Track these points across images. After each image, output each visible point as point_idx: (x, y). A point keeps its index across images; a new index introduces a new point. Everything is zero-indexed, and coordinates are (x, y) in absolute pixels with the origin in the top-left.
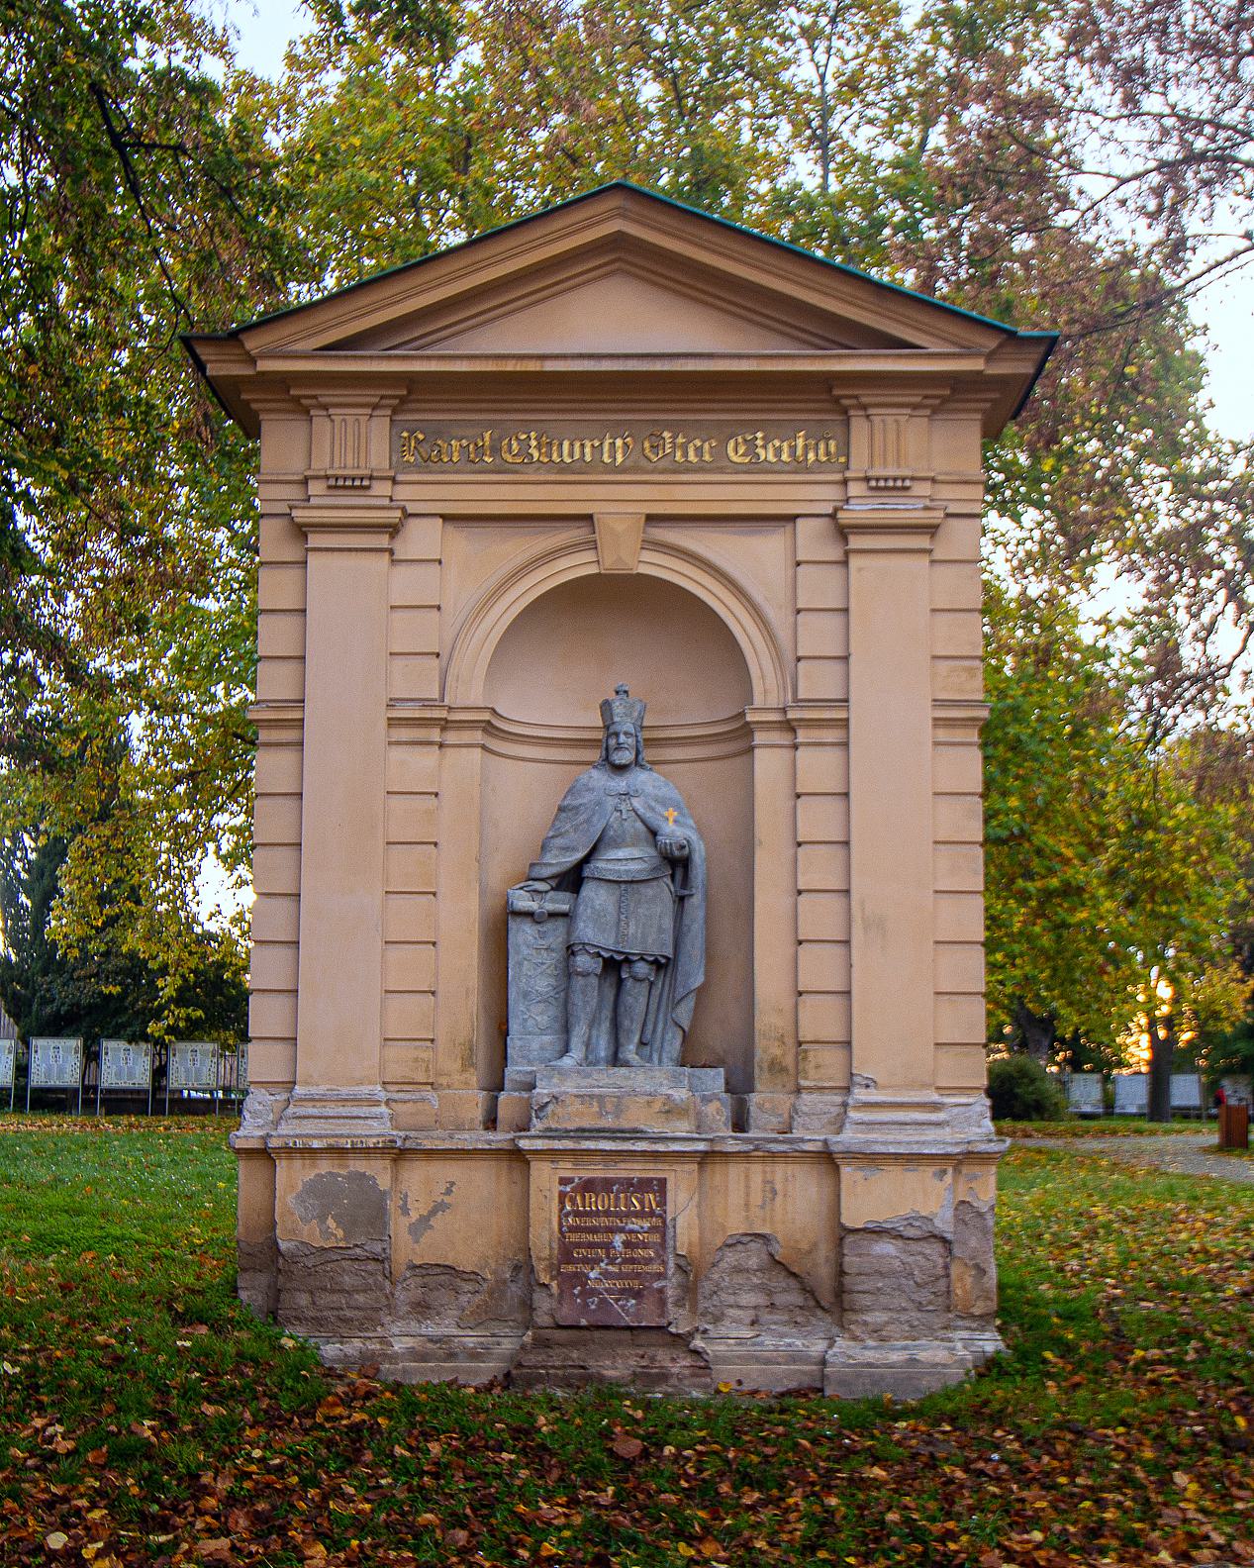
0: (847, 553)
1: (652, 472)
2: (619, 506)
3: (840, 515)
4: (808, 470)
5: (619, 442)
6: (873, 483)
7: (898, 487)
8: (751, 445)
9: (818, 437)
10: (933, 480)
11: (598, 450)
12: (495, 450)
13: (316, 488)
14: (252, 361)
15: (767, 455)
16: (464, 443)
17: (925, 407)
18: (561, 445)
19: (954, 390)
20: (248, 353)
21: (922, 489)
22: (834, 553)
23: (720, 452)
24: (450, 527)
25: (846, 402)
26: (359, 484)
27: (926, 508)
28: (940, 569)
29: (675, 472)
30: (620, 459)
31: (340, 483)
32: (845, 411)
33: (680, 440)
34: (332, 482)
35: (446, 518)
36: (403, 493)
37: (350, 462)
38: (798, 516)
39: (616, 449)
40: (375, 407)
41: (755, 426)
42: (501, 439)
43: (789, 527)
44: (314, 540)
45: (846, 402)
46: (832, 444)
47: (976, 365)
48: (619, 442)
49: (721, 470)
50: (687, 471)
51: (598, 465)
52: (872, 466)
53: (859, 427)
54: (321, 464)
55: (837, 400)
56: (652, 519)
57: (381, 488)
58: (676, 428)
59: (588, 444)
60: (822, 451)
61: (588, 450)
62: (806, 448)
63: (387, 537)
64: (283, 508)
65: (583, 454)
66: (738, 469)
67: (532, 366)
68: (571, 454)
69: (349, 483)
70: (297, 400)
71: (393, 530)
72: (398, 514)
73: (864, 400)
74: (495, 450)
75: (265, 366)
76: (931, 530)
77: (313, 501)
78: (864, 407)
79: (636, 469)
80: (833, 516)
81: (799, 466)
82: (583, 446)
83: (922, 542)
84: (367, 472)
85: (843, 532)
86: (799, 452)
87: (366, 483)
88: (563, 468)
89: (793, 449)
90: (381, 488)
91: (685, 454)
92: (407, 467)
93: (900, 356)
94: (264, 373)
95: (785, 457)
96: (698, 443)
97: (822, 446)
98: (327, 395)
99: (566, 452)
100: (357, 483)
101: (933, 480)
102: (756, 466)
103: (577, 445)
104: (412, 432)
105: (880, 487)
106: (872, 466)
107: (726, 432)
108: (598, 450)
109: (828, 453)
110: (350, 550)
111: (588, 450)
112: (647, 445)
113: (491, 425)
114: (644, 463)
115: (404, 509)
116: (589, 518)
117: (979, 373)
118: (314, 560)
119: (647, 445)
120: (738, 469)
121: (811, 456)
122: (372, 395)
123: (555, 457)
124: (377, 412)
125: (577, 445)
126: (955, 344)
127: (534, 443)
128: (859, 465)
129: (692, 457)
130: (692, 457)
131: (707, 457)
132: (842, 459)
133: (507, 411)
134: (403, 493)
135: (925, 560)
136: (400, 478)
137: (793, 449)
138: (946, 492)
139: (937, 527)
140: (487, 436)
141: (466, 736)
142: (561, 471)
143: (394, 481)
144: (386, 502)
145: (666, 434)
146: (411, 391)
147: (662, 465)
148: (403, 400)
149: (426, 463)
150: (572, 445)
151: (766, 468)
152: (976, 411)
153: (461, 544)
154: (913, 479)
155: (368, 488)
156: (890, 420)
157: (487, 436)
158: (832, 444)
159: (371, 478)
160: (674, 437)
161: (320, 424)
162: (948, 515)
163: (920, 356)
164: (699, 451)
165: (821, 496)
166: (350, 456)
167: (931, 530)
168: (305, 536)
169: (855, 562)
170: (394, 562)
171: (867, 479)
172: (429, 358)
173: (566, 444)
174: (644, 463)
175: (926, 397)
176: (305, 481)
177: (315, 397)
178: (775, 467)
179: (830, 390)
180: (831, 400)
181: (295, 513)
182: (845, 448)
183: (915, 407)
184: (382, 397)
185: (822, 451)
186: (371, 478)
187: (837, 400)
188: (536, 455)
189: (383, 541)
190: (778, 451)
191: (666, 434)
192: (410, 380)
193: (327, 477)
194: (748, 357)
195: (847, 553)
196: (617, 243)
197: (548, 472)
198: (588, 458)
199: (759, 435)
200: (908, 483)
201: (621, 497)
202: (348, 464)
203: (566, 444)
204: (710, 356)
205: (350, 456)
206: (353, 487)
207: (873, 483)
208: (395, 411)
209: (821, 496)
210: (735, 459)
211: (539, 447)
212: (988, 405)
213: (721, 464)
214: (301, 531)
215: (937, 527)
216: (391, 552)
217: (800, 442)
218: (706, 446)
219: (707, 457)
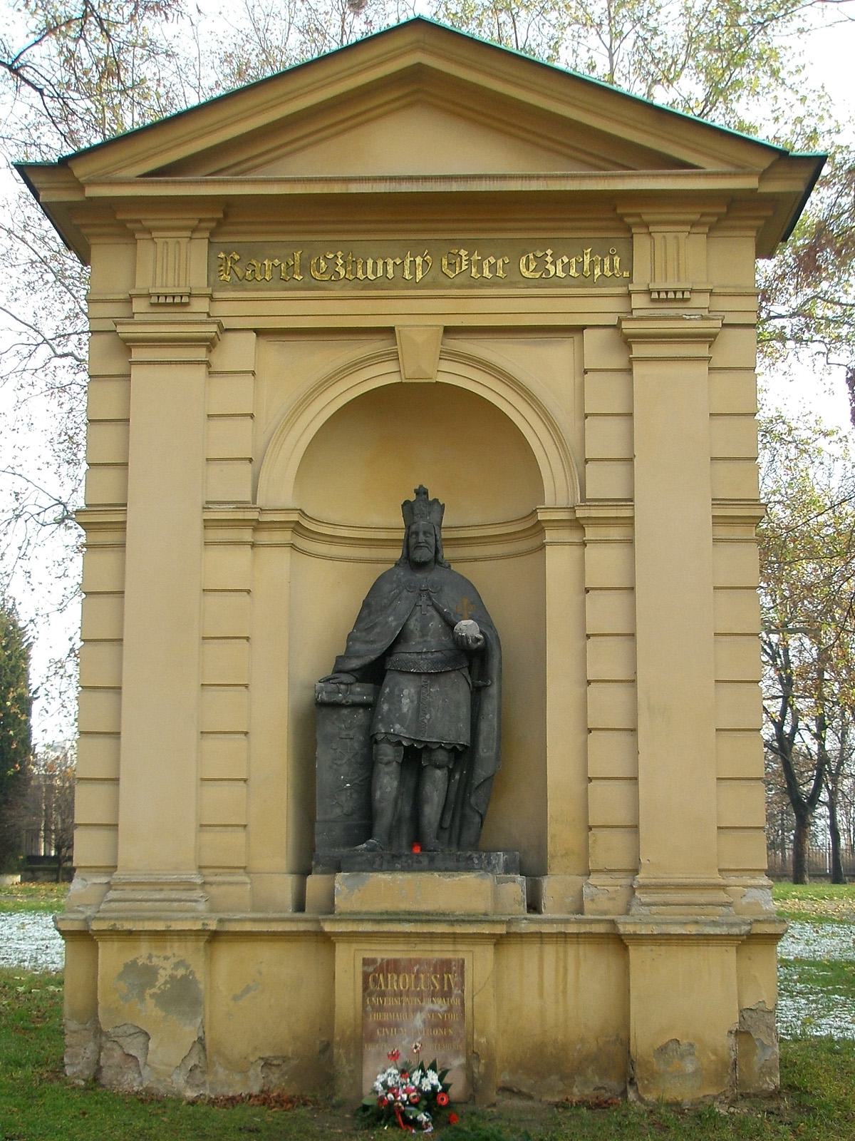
0: (631, 361)
1: (450, 287)
2: (418, 318)
3: (624, 325)
4: (594, 285)
5: (419, 260)
6: (655, 295)
7: (679, 298)
8: (541, 261)
9: (602, 251)
10: (711, 293)
11: (399, 267)
12: (305, 269)
13: (139, 306)
14: (81, 187)
15: (556, 270)
16: (277, 262)
17: (703, 224)
18: (365, 263)
19: (729, 207)
20: (77, 180)
21: (701, 301)
22: (618, 361)
23: (512, 268)
24: (263, 341)
25: (629, 220)
26: (176, 302)
27: (703, 318)
28: (719, 378)
29: (471, 287)
30: (419, 275)
31: (162, 300)
32: (628, 229)
33: (476, 257)
34: (154, 300)
35: (259, 332)
36: (221, 309)
37: (170, 282)
38: (584, 327)
39: (416, 267)
40: (194, 230)
41: (545, 243)
42: (310, 258)
43: (577, 337)
44: (138, 354)
45: (629, 220)
46: (617, 260)
47: (749, 183)
48: (419, 260)
49: (513, 285)
50: (482, 286)
51: (398, 281)
52: (653, 279)
53: (641, 245)
54: (143, 284)
55: (620, 218)
56: (448, 331)
57: (200, 305)
58: (471, 246)
59: (390, 262)
60: (607, 266)
61: (390, 268)
62: (592, 263)
63: (204, 350)
64: (109, 325)
65: (385, 271)
66: (529, 283)
67: (337, 189)
68: (375, 272)
69: (169, 300)
70: (122, 224)
71: (210, 344)
72: (214, 328)
73: (646, 218)
74: (305, 269)
75: (92, 192)
76: (709, 338)
77: (636, 314)
78: (647, 225)
79: (435, 285)
80: (617, 327)
81: (585, 280)
82: (375, 263)
83: (702, 350)
84: (187, 290)
85: (627, 341)
86: (586, 267)
87: (185, 300)
88: (368, 284)
89: (580, 265)
90: (200, 305)
91: (480, 270)
92: (224, 286)
93: (678, 176)
94: (91, 199)
95: (573, 272)
96: (493, 261)
97: (607, 262)
98: (150, 220)
99: (370, 270)
100: (177, 300)
101: (711, 293)
102: (546, 281)
103: (380, 263)
104: (228, 253)
105: (658, 297)
106: (653, 279)
107: (519, 249)
108: (399, 267)
109: (612, 268)
110: (170, 363)
111: (390, 268)
112: (445, 262)
113: (300, 245)
114: (442, 279)
115: (220, 324)
116: (390, 330)
117: (753, 191)
118: (136, 372)
119: (445, 262)
120: (529, 283)
121: (597, 271)
122: (190, 219)
123: (360, 274)
124: (197, 235)
125: (380, 263)
126: (728, 163)
127: (340, 262)
128: (639, 283)
129: (486, 273)
130: (486, 273)
131: (500, 273)
132: (626, 274)
133: (316, 232)
134: (221, 309)
135: (704, 367)
136: (217, 295)
137: (580, 265)
138: (723, 304)
139: (715, 336)
140: (297, 255)
141: (603, 532)
142: (365, 288)
143: (212, 298)
144: (204, 317)
145: (463, 252)
146: (223, 218)
147: (457, 280)
148: (220, 223)
149: (240, 283)
150: (375, 263)
151: (555, 282)
152: (751, 228)
153: (275, 355)
154: (692, 291)
155: (187, 304)
156: (670, 236)
157: (297, 255)
158: (617, 260)
159: (190, 295)
160: (470, 255)
161: (144, 248)
162: (724, 325)
163: (700, 175)
164: (493, 268)
165: (603, 308)
166: (171, 274)
167: (709, 338)
168: (129, 350)
169: (638, 369)
170: (211, 374)
171: (649, 292)
172: (254, 182)
173: (370, 262)
174: (442, 279)
175: (703, 215)
176: (129, 301)
177: (139, 221)
178: (566, 282)
179: (615, 210)
180: (613, 218)
181: (119, 329)
182: (628, 264)
183: (693, 224)
184: (201, 220)
185: (607, 266)
186: (190, 295)
187: (620, 218)
188: (342, 273)
189: (201, 354)
190: (566, 267)
191: (463, 252)
192: (228, 204)
193: (149, 296)
194: (538, 177)
195: (631, 361)
196: (416, 75)
197: (354, 289)
198: (390, 275)
199: (549, 252)
200: (687, 295)
201: (420, 313)
202: (169, 284)
203: (370, 262)
204: (503, 177)
205: (171, 274)
206: (174, 304)
207: (655, 295)
208: (213, 233)
209: (603, 308)
210: (526, 274)
211: (344, 266)
212: (760, 223)
213: (514, 279)
214: (627, 341)
215: (715, 336)
216: (208, 364)
217: (587, 259)
218: (500, 263)
219: (500, 273)
